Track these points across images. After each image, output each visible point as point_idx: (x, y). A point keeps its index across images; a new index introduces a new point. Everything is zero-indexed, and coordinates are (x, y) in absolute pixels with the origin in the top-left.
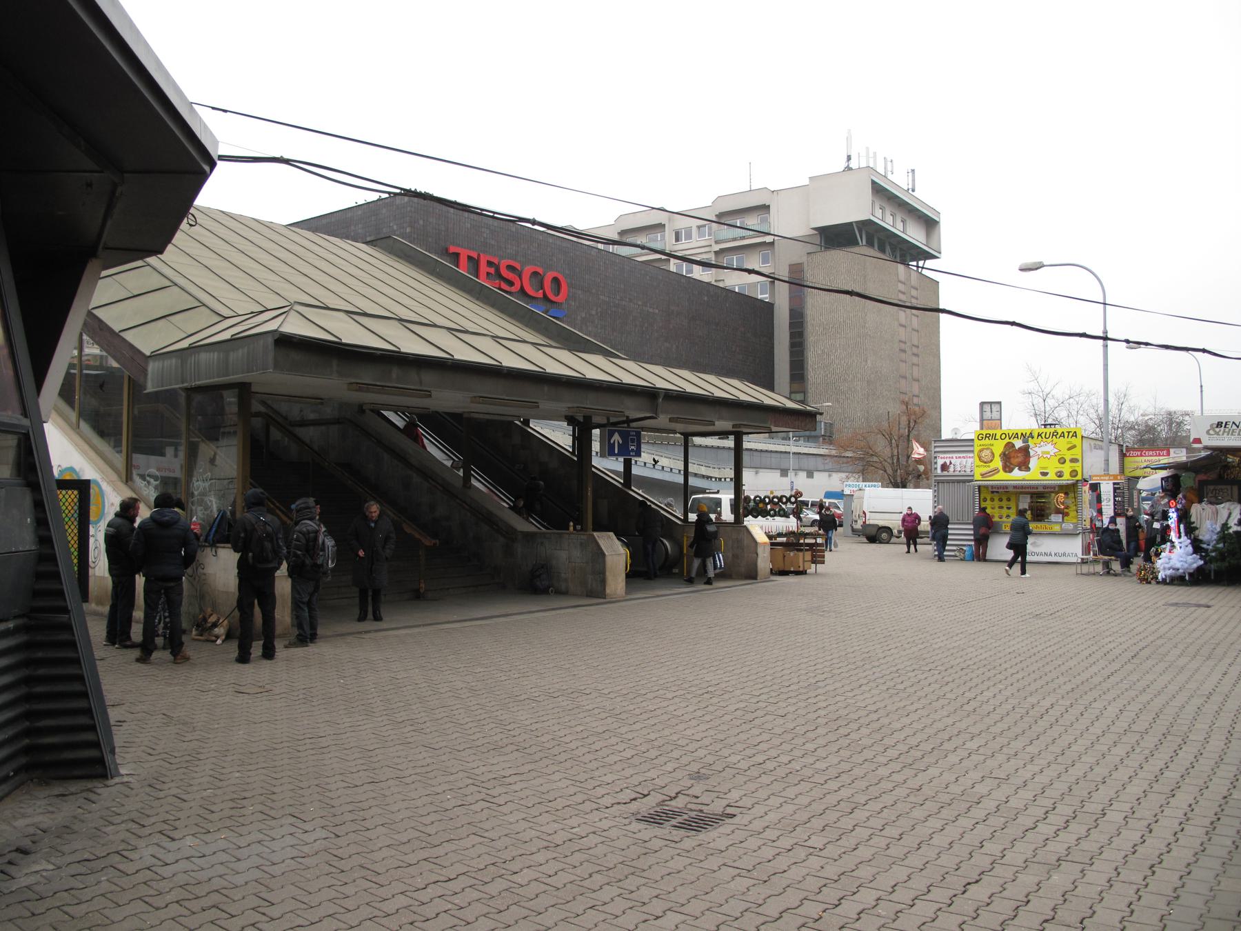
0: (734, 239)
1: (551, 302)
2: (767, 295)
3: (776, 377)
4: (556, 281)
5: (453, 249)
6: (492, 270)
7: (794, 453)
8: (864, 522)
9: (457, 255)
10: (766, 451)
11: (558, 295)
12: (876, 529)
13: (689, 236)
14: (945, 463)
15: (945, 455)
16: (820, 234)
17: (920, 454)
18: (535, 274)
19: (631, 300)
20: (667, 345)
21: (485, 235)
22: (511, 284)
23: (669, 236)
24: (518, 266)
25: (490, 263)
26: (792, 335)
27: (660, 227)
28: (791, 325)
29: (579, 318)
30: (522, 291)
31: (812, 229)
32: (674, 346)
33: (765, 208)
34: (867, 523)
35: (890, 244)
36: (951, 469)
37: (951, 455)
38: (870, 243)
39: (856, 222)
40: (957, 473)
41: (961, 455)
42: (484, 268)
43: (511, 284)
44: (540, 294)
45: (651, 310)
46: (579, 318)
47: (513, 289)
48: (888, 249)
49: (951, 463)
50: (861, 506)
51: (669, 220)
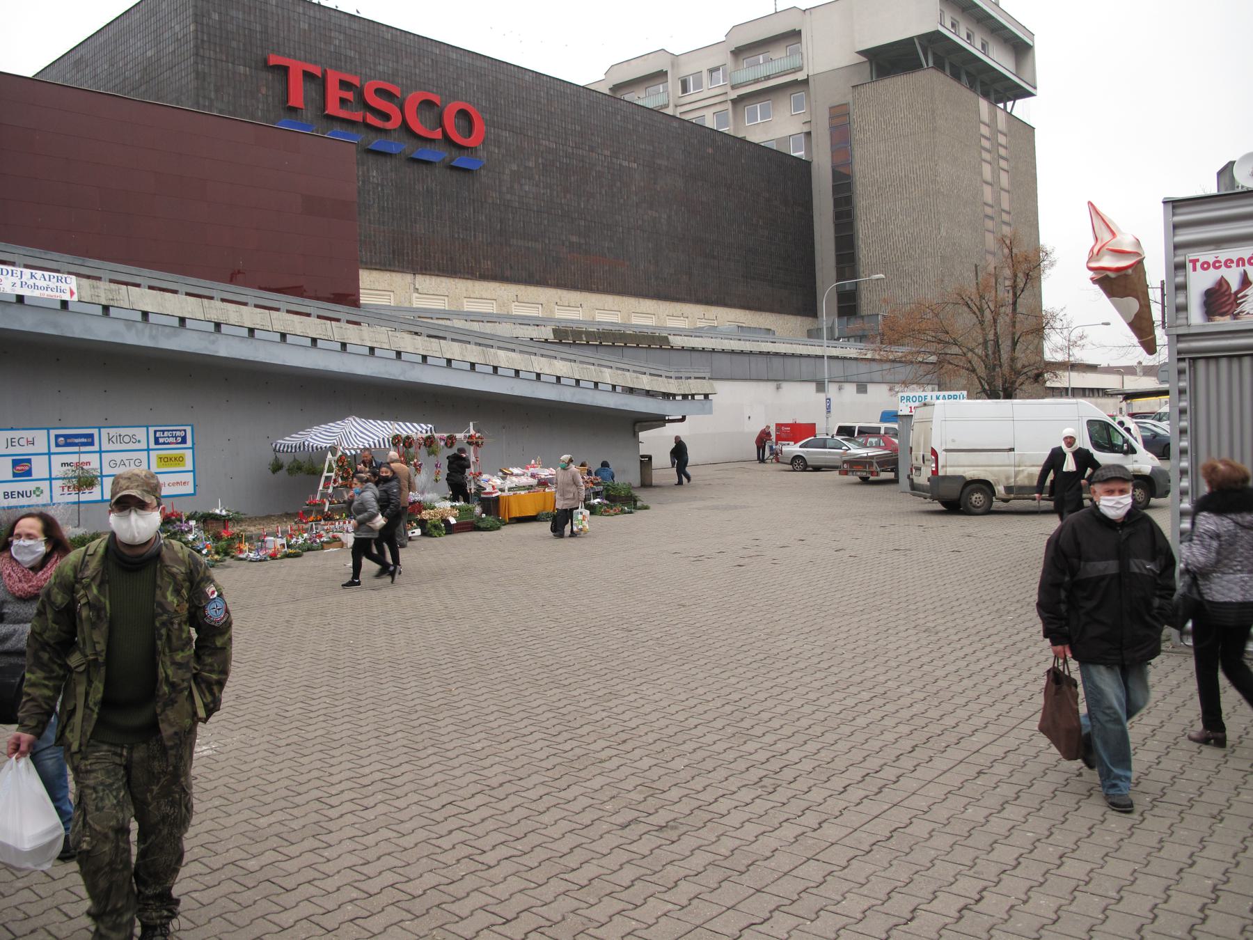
0: (757, 81)
1: (461, 148)
2: (803, 153)
4: (464, 114)
5: (274, 60)
6: (349, 95)
7: (830, 357)
8: (935, 473)
9: (284, 70)
10: (793, 355)
12: (958, 486)
13: (699, 85)
14: (1222, 283)
15: (1224, 254)
16: (871, 61)
18: (428, 104)
19: (592, 149)
22: (387, 117)
23: (673, 85)
24: (397, 92)
25: (345, 85)
26: (837, 203)
27: (660, 75)
29: (507, 171)
30: (405, 127)
31: (861, 53)
32: (665, 216)
33: (795, 35)
34: (941, 473)
35: (968, 74)
38: (939, 66)
39: (919, 37)
42: (334, 92)
44: (437, 134)
45: (625, 164)
46: (507, 171)
47: (388, 125)
48: (964, 78)
50: (927, 439)
51: (673, 65)
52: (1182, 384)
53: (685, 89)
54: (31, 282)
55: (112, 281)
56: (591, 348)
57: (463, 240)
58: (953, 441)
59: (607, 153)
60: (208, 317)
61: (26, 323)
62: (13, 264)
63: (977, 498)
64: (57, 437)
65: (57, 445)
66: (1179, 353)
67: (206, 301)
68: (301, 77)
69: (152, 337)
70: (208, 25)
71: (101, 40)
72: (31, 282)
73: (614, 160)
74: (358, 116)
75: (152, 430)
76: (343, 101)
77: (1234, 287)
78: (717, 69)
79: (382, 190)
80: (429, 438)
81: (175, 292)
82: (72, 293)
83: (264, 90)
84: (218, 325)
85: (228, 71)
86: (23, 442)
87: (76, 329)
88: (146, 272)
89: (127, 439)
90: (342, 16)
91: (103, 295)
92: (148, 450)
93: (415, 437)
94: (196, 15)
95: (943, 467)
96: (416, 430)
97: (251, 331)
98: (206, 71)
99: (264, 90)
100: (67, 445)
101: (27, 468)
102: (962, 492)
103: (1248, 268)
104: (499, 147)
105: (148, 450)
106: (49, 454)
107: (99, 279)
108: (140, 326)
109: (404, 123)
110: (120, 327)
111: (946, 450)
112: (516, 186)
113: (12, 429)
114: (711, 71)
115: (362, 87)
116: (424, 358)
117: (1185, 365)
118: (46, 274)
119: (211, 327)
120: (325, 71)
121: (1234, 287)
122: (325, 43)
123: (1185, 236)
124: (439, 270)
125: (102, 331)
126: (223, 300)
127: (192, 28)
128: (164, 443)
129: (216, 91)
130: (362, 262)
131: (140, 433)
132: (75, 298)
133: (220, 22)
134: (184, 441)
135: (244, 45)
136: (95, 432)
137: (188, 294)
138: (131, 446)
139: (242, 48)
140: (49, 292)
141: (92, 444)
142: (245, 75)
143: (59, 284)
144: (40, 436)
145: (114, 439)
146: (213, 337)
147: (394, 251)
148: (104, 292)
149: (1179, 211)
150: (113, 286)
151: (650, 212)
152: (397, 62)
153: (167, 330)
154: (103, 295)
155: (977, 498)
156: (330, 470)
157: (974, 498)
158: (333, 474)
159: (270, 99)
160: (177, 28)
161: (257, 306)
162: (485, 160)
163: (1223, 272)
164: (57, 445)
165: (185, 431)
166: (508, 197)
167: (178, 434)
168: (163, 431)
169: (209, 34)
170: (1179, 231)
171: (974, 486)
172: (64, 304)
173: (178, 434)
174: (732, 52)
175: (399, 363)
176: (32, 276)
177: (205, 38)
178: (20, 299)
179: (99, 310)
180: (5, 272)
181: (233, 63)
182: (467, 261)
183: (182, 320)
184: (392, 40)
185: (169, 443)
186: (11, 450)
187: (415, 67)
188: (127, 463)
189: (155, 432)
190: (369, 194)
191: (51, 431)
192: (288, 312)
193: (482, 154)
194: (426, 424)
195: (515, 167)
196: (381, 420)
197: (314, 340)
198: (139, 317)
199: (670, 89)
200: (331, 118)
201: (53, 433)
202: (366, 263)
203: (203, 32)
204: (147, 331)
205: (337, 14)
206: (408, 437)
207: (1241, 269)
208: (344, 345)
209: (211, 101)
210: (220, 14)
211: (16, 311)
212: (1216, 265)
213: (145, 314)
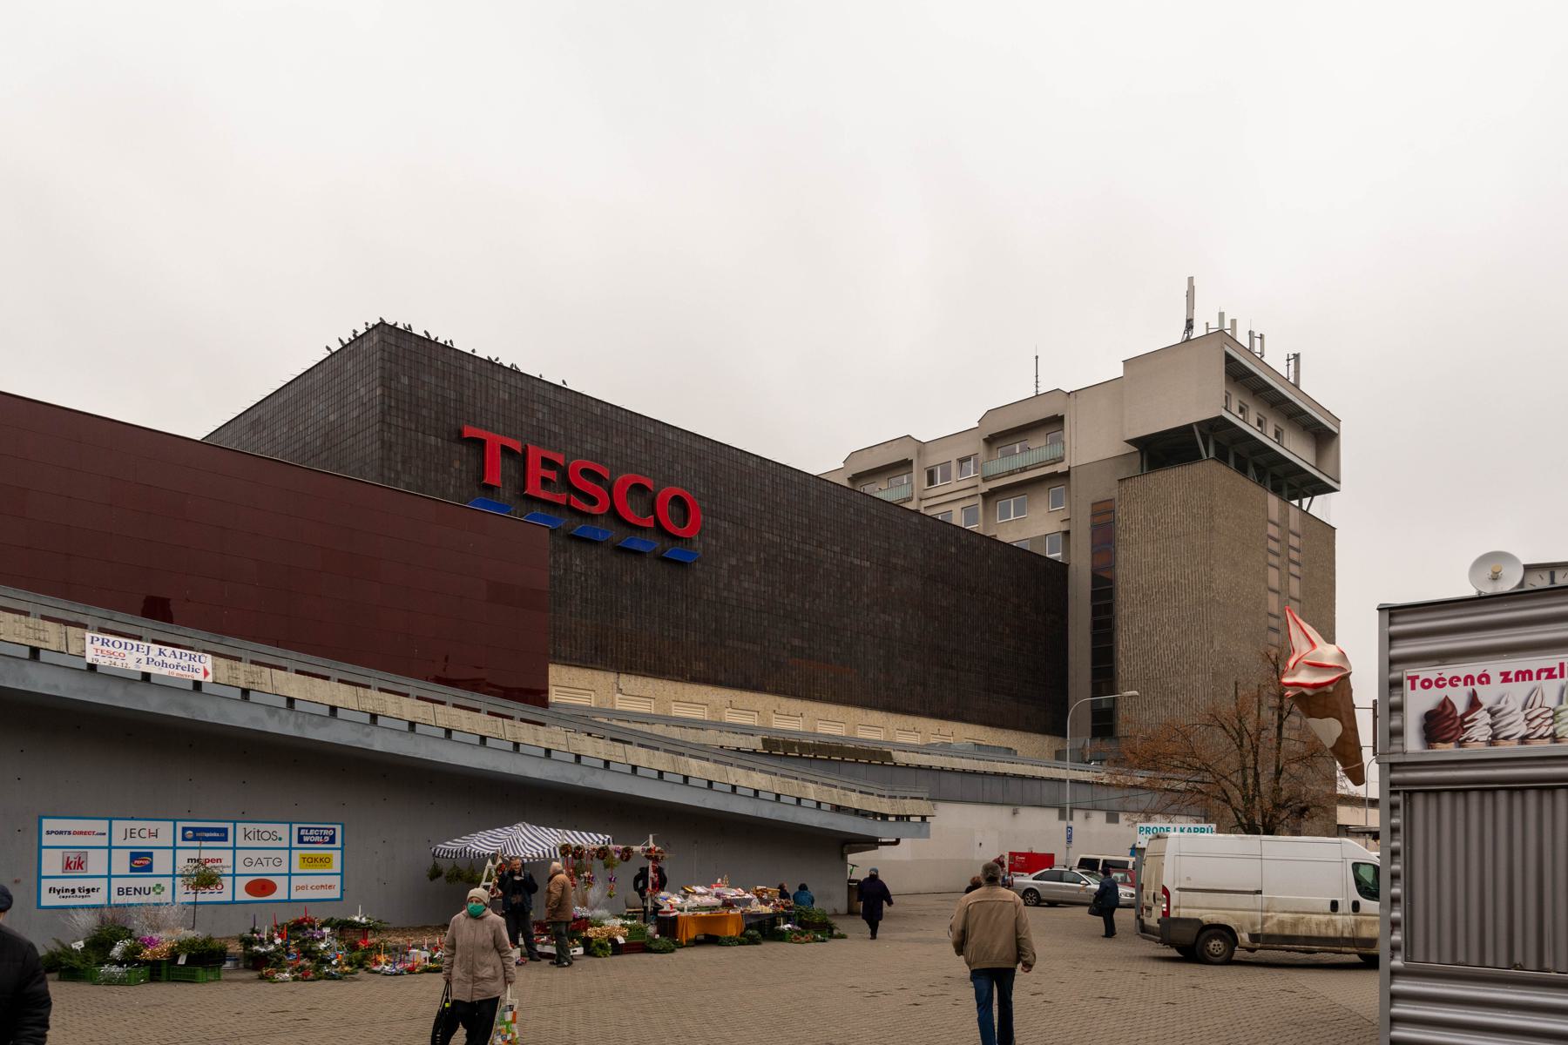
0: (1011, 473)
1: (674, 538)
2: (1059, 554)
3: (1071, 673)
4: (678, 501)
5: (470, 431)
7: (1071, 781)
8: (1166, 914)
9: (481, 443)
10: (1033, 778)
11: (685, 526)
12: (1193, 932)
13: (946, 477)
14: (1446, 704)
15: (1449, 671)
17: (1318, 667)
18: (640, 488)
19: (820, 545)
20: (888, 618)
21: (540, 416)
25: (548, 463)
26: (1096, 611)
27: (906, 464)
28: (1095, 595)
29: (725, 566)
30: (614, 514)
32: (898, 621)
34: (1173, 915)
36: (1480, 729)
37: (1474, 668)
40: (1509, 748)
41: (1534, 663)
42: (536, 471)
43: (592, 501)
44: (648, 522)
45: (857, 562)
46: (725, 566)
47: (594, 510)
49: (1474, 704)
50: (1159, 876)
51: (919, 453)
52: (1394, 821)
53: (931, 481)
54: (159, 659)
55: (252, 662)
56: (804, 761)
57: (673, 638)
58: (1188, 879)
59: (837, 549)
60: (363, 706)
61: (152, 703)
62: (140, 638)
63: (1216, 945)
64: (185, 829)
65: (184, 839)
66: (1392, 784)
67: (361, 690)
68: (498, 452)
69: (299, 726)
70: (396, 389)
71: (281, 400)
72: (159, 659)
73: (844, 557)
74: (561, 497)
75: (295, 827)
76: (545, 482)
77: (1461, 710)
78: (968, 459)
79: (586, 580)
80: (602, 849)
81: (327, 678)
82: (206, 673)
83: (457, 464)
84: (374, 717)
85: (417, 441)
86: (143, 833)
87: (207, 712)
88: (294, 655)
89: (266, 836)
90: (546, 386)
91: (242, 677)
92: (290, 849)
93: (586, 847)
94: (382, 377)
95: (1175, 907)
96: (589, 840)
97: (412, 725)
98: (393, 440)
99: (457, 464)
100: (195, 839)
101: (147, 862)
102: (1198, 937)
103: (1477, 686)
104: (717, 540)
105: (290, 849)
106: (175, 848)
107: (240, 659)
108: (284, 713)
109: (612, 505)
110: (261, 713)
111: (1180, 889)
112: (734, 583)
113: (132, 819)
114: (961, 461)
115: (567, 466)
116: (607, 763)
117: (1399, 799)
118: (178, 651)
119: (367, 719)
120: (526, 446)
121: (1461, 710)
122: (527, 416)
123: (1402, 649)
124: (646, 670)
125: (239, 717)
126: (381, 690)
127: (379, 392)
128: (309, 842)
129: (404, 462)
130: (560, 657)
131: (282, 830)
132: (210, 679)
133: (410, 386)
134: (332, 840)
135: (436, 413)
136: (230, 826)
137: (340, 681)
138: (271, 844)
139: (433, 416)
140: (180, 671)
141: (225, 839)
142: (437, 447)
143: (192, 663)
144: (165, 829)
145: (251, 835)
146: (367, 730)
147: (596, 648)
148: (243, 674)
149: (1397, 619)
150: (255, 668)
151: (882, 616)
152: (607, 440)
153: (316, 719)
154: (242, 677)
155: (1216, 945)
156: (488, 880)
157: (1211, 945)
158: (491, 884)
159: (464, 475)
160: (363, 391)
161: (419, 698)
162: (700, 552)
163: (1448, 691)
164: (184, 839)
165: (334, 829)
166: (725, 594)
167: (326, 832)
168: (309, 829)
169: (397, 400)
170: (1397, 643)
171: (1213, 931)
172: (197, 685)
173: (326, 832)
174: (984, 440)
175: (577, 768)
176: (161, 652)
177: (393, 404)
178: (146, 677)
179: (237, 694)
180: (129, 647)
181: (424, 433)
182: (677, 661)
183: (333, 709)
184: (602, 416)
185: (314, 843)
186: (129, 842)
188: (264, 862)
189: (300, 829)
190: (571, 584)
191: (178, 823)
192: (455, 706)
193: (698, 546)
194: (603, 834)
195: (734, 562)
196: (555, 828)
197: (483, 739)
198: (283, 703)
199: (915, 481)
200: (531, 499)
201: (180, 825)
202: (565, 659)
203: (390, 397)
204: (292, 719)
205: (541, 384)
206: (578, 848)
207: (1470, 688)
208: (517, 745)
209: (397, 473)
210: (410, 378)
211: (141, 689)
212: (1440, 683)
213: (291, 701)
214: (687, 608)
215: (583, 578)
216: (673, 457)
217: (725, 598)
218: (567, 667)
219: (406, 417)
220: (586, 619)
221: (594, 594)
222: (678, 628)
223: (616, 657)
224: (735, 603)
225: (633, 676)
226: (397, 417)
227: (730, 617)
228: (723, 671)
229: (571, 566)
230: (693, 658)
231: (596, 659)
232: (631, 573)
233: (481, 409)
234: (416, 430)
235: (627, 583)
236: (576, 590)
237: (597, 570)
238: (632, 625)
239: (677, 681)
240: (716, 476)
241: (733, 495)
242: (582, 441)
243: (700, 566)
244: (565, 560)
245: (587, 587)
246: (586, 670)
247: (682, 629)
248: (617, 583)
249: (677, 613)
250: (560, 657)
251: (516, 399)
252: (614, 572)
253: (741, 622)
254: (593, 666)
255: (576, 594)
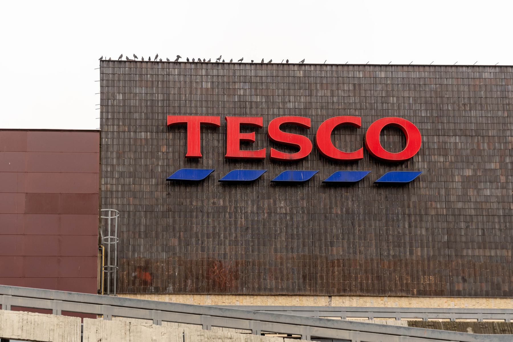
44: (359, 154)
57: (394, 256)
79: (292, 219)
104: (445, 155)
122: (229, 95)
124: (362, 290)
129: (118, 158)
130: (265, 289)
133: (124, 100)
142: (146, 139)
147: (304, 277)
159: (171, 155)
162: (424, 172)
166: (460, 205)
181: (135, 132)
182: (401, 278)
187: (332, 96)
190: (275, 225)
195: (468, 172)
202: (271, 290)
209: (113, 165)
214: (410, 226)
215: (288, 218)
216: (387, 91)
217: (459, 209)
218: (273, 297)
219: (121, 124)
220: (292, 252)
221: (300, 229)
222: (399, 246)
223: (328, 282)
224: (473, 212)
225: (348, 298)
226: (113, 125)
227: (467, 227)
228: (461, 281)
229: (276, 209)
230: (421, 273)
231: (305, 287)
232: (342, 205)
233: (186, 101)
234: (129, 131)
235: (337, 213)
236: (281, 229)
237: (302, 208)
238: (343, 251)
239: (402, 297)
240: (442, 97)
241: (465, 110)
242: (284, 103)
243: (425, 185)
244: (269, 205)
245: (293, 225)
246: (294, 297)
247: (405, 247)
248: (326, 217)
249: (399, 233)
250: (265, 289)
251: (218, 85)
252: (322, 206)
253: (483, 229)
254: (301, 293)
255: (281, 232)
